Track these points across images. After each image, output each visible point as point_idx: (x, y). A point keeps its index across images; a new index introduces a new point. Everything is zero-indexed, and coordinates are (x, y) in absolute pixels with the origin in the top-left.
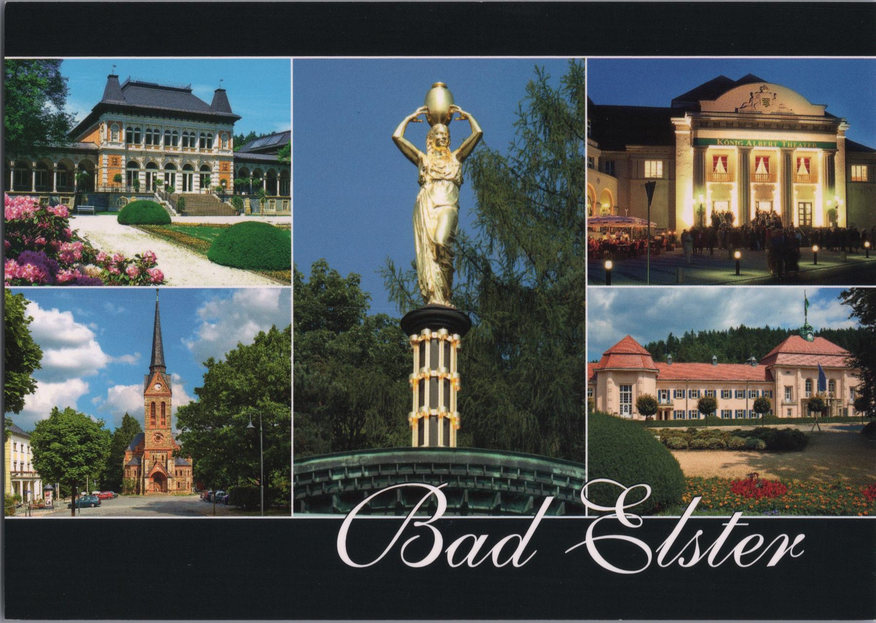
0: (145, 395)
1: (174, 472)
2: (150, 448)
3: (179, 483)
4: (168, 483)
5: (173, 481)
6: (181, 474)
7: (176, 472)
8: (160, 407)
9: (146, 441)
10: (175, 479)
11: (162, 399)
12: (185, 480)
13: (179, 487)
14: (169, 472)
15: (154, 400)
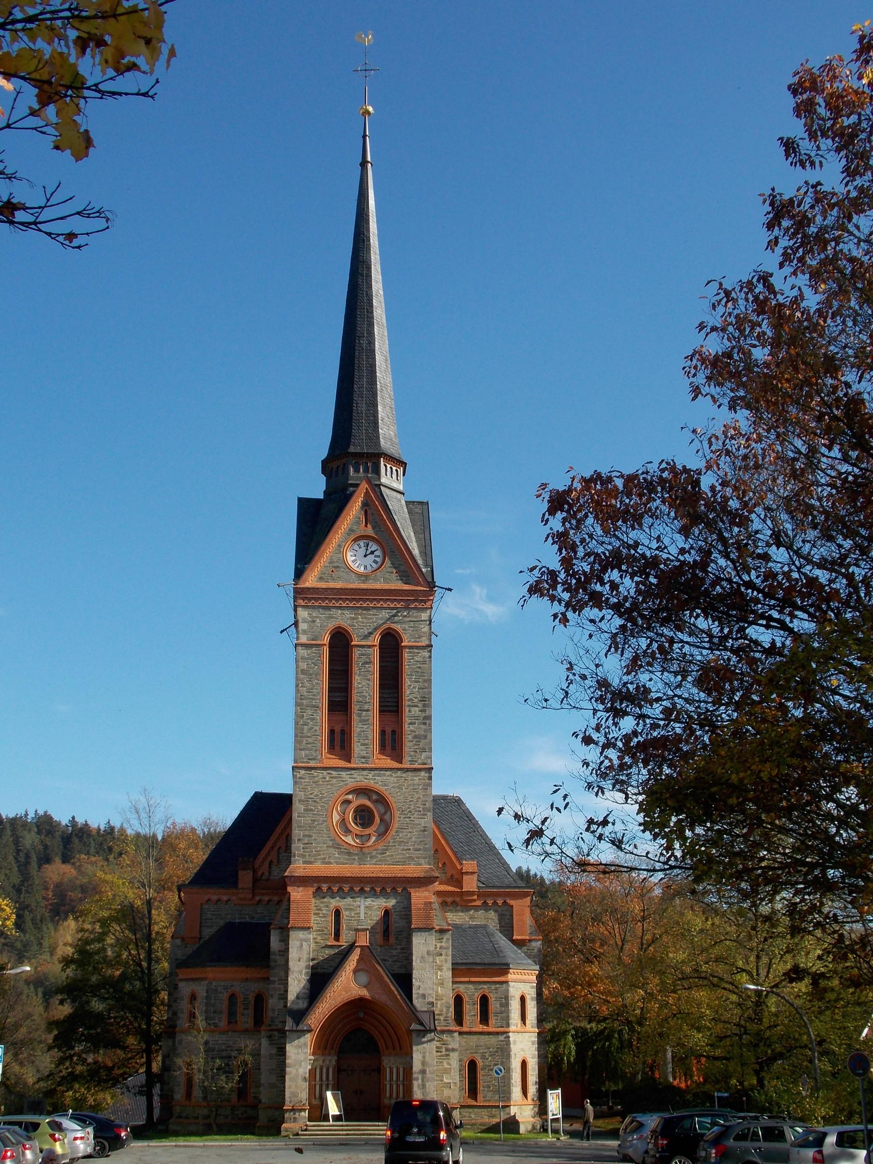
0: (300, 594)
1: (445, 1008)
2: (318, 869)
3: (473, 1065)
4: (417, 1066)
5: (445, 1052)
6: (485, 1018)
7: (459, 1000)
8: (375, 654)
9: (296, 833)
10: (455, 1041)
11: (380, 617)
12: (504, 1051)
13: (473, 1092)
14: (417, 1002)
15: (343, 618)
